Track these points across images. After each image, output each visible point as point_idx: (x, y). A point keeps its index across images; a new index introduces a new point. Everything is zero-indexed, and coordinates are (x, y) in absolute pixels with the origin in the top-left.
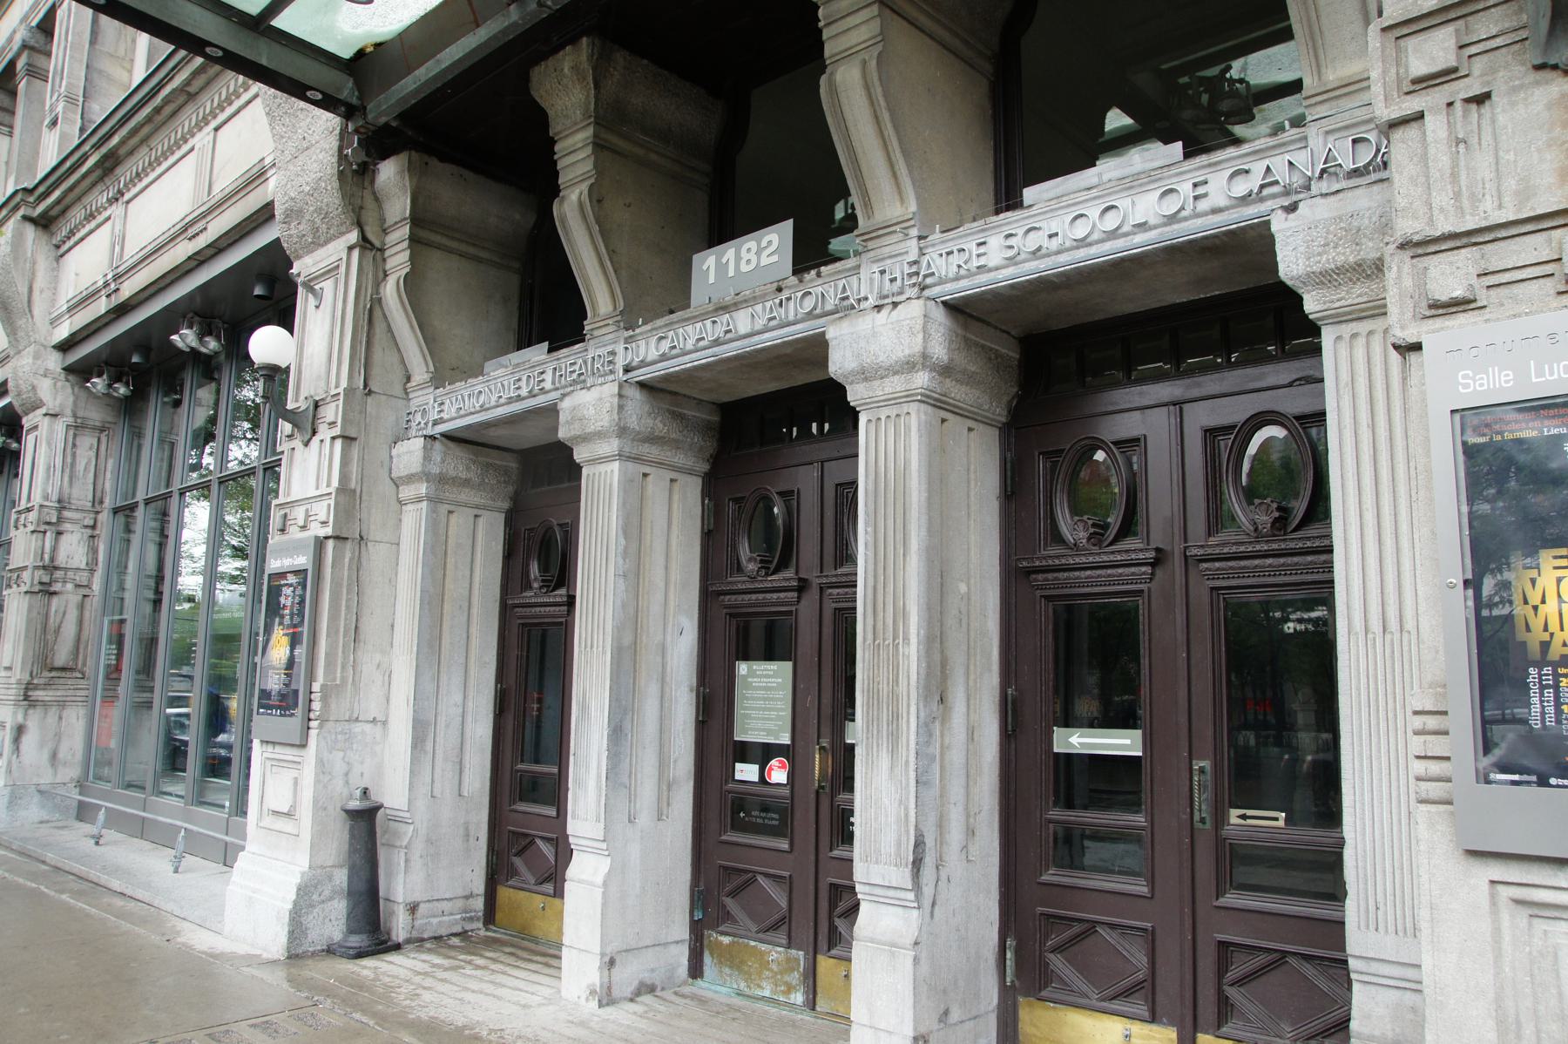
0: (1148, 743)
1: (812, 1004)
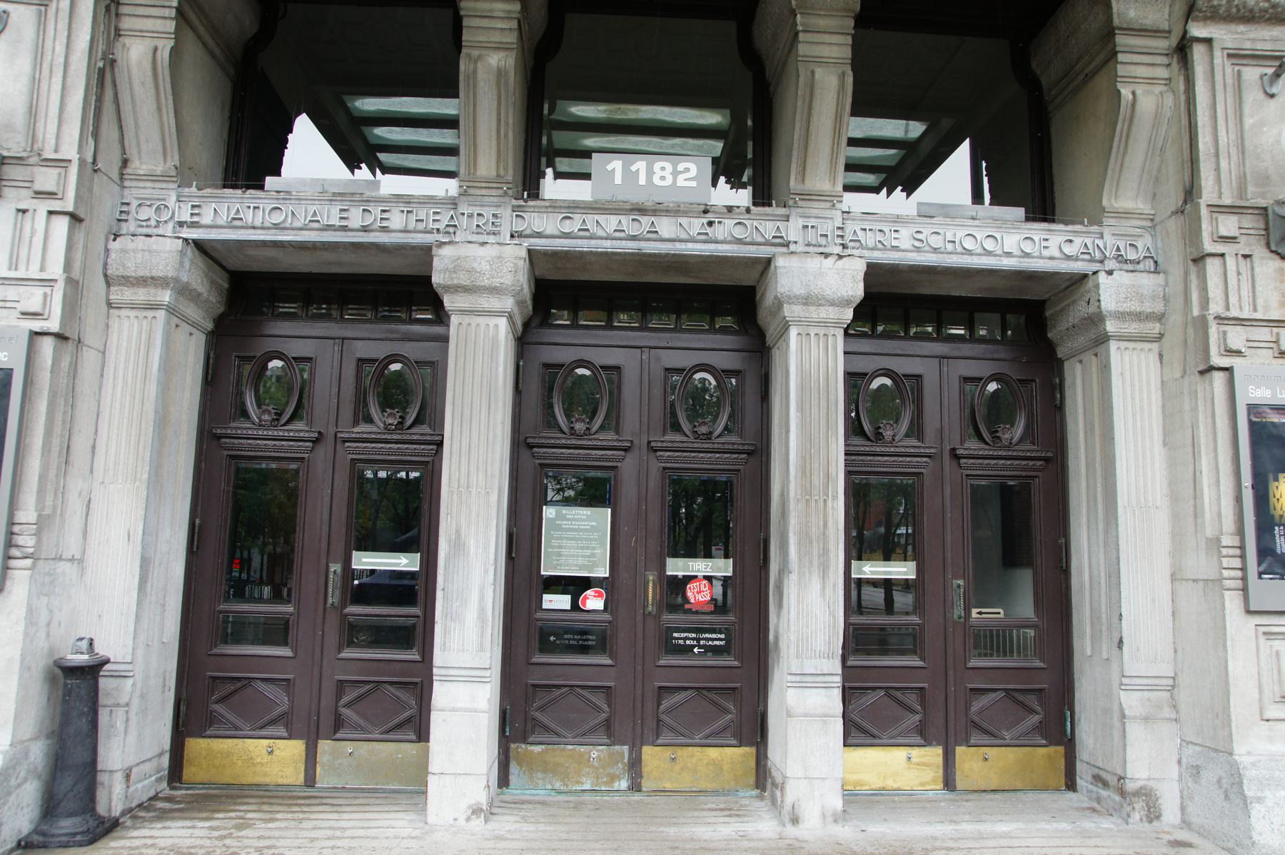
0: (920, 571)
1: (635, 787)
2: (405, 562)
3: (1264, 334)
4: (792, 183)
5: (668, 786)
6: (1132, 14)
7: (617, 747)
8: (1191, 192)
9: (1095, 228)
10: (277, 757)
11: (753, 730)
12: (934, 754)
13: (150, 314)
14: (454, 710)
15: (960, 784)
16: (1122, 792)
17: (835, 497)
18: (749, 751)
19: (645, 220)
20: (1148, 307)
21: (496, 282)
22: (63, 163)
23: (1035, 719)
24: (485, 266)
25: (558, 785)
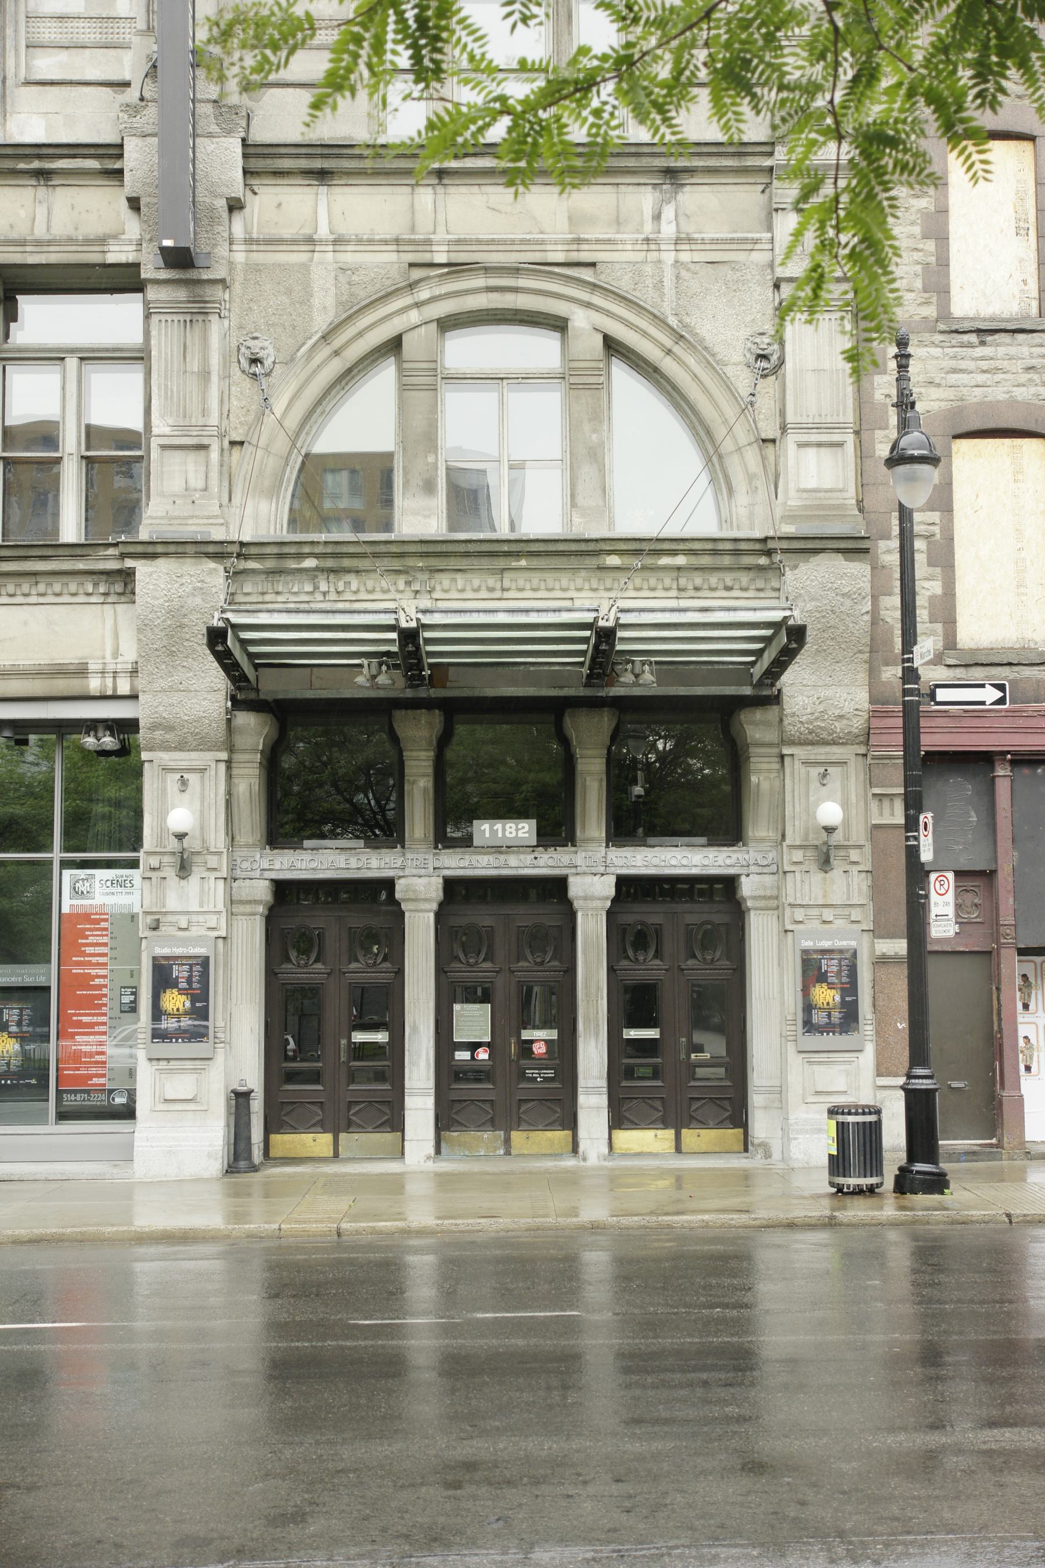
1: (508, 1153)
2: (381, 1037)
3: (815, 912)
6: (757, 736)
8: (783, 836)
10: (320, 1142)
11: (570, 1122)
15: (684, 1150)
18: (569, 1133)
19: (502, 857)
20: (768, 893)
21: (428, 896)
22: (220, 853)
23: (727, 1114)
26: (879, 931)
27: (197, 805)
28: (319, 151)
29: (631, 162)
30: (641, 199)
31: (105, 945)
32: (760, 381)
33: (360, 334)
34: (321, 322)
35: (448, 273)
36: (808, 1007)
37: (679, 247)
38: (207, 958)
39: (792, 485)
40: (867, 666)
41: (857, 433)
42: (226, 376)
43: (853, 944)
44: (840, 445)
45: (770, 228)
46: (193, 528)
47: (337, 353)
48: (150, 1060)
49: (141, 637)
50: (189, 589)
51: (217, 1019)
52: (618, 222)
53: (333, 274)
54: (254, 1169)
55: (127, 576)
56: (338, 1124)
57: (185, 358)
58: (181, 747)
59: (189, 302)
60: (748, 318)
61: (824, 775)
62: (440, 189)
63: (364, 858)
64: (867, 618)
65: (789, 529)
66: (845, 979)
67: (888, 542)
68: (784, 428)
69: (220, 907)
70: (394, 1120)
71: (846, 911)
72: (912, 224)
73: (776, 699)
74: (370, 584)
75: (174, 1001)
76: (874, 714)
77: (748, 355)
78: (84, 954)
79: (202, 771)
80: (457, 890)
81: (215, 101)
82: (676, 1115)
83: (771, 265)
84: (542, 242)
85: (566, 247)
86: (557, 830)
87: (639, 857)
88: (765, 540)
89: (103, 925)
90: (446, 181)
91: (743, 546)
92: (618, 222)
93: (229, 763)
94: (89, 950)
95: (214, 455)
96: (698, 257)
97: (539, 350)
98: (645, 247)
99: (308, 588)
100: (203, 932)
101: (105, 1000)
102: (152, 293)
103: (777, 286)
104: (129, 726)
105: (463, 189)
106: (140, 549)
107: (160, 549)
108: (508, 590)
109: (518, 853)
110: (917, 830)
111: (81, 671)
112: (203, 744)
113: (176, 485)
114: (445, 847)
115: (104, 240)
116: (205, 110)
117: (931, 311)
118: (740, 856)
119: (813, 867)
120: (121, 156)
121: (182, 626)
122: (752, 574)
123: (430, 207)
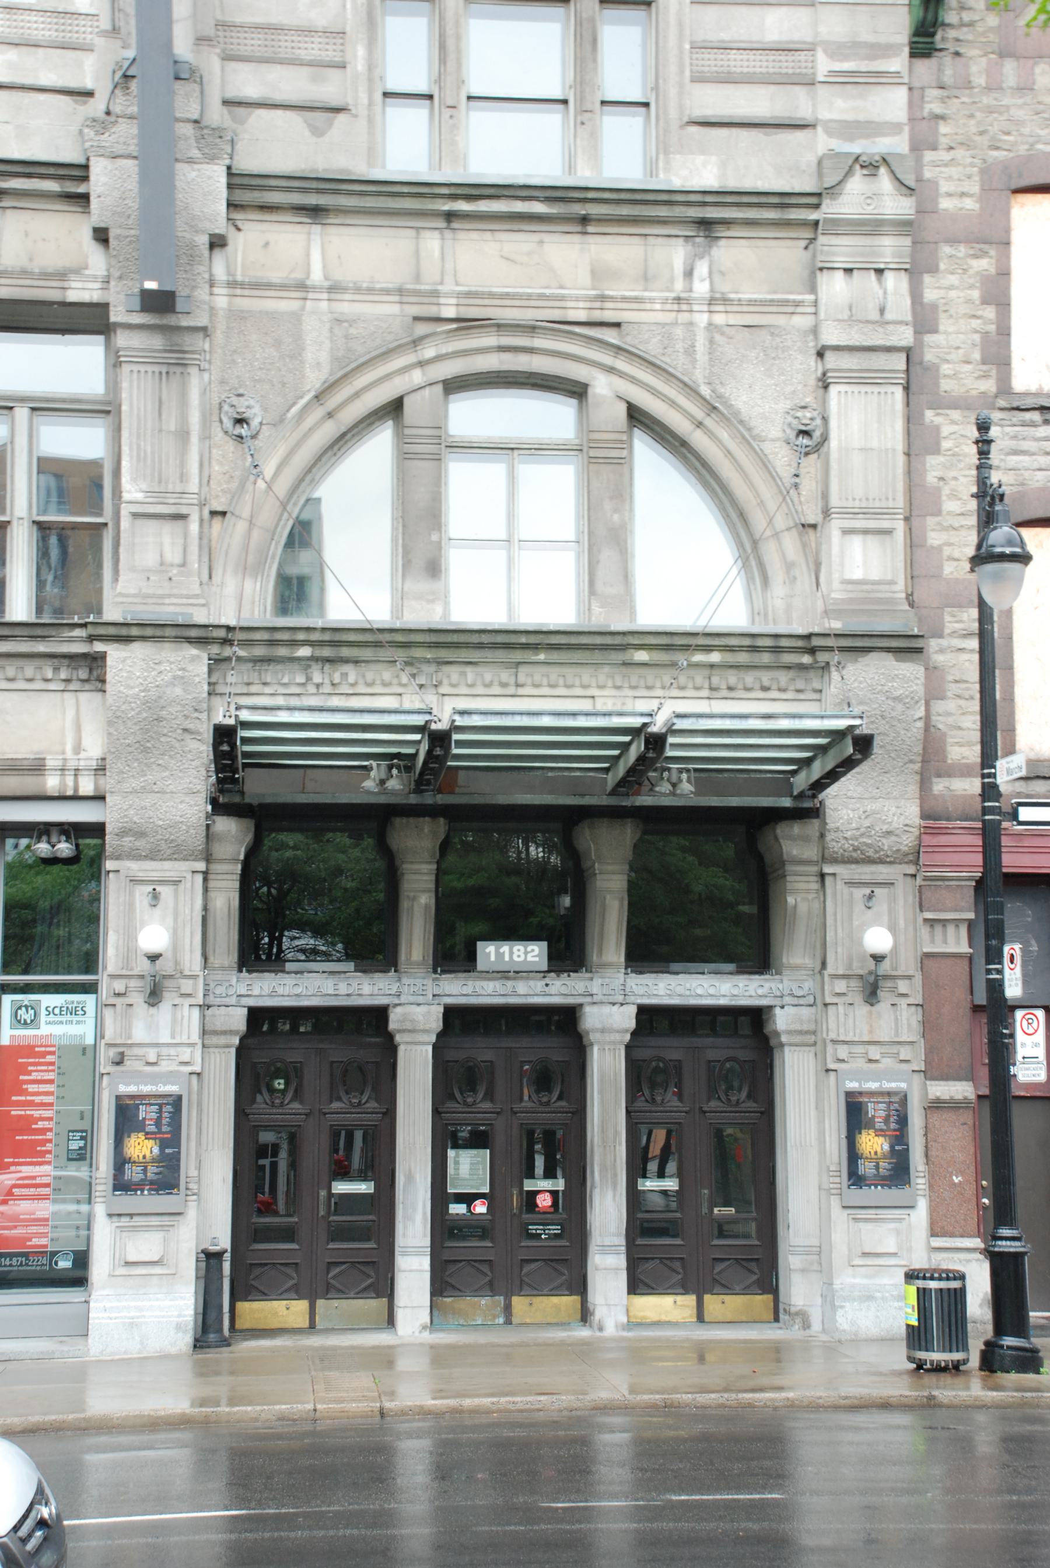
0: (681, 1185)
1: (508, 1322)
3: (860, 1049)
4: (595, 958)
5: (528, 1321)
6: (795, 852)
7: (497, 1298)
8: (824, 964)
9: (778, 977)
10: (292, 1311)
11: (579, 1285)
12: (691, 1300)
13: (227, 1050)
14: (411, 1271)
15: (707, 1318)
16: (790, 1314)
17: (620, 1144)
18: (576, 1299)
19: (510, 983)
20: (805, 1027)
21: (427, 1027)
22: (194, 977)
23: (755, 1277)
24: (421, 1018)
25: (462, 1322)
26: (932, 1072)
27: (170, 920)
28: (314, 185)
29: (662, 212)
30: (673, 253)
31: (51, 1082)
32: (805, 462)
33: (357, 395)
34: (314, 379)
35: (457, 329)
36: (853, 1155)
37: (713, 308)
38: (180, 1098)
39: (836, 576)
40: (918, 777)
41: (907, 519)
42: (206, 437)
43: (903, 1085)
44: (888, 532)
45: (813, 289)
46: (171, 609)
47: (330, 415)
48: (110, 1215)
49: (112, 730)
50: (167, 677)
51: (188, 1168)
52: (646, 278)
53: (328, 326)
54: (226, 1343)
55: (96, 661)
56: (314, 1288)
57: (160, 415)
58: (152, 856)
59: (166, 351)
60: (789, 389)
61: (870, 897)
62: (448, 234)
63: (355, 984)
64: (920, 724)
65: (837, 625)
66: (893, 1126)
67: (940, 641)
68: (826, 513)
69: (195, 1038)
70: (381, 1283)
71: (894, 1049)
72: (971, 287)
73: (816, 813)
74: (370, 676)
75: (141, 1147)
76: (927, 831)
77: (788, 431)
78: (25, 1092)
79: (176, 883)
80: (459, 1020)
81: (196, 122)
82: (696, 1279)
83: (815, 331)
84: (562, 298)
85: (588, 305)
86: (568, 953)
87: (661, 985)
88: (809, 637)
89: (49, 1058)
90: (454, 225)
91: (784, 642)
92: (646, 278)
93: (206, 874)
94: (32, 1088)
95: (194, 527)
96: (733, 319)
97: (551, 417)
98: (676, 307)
99: (300, 679)
100: (174, 1067)
101: (49, 1146)
102: (122, 339)
103: (820, 354)
104: (98, 830)
105: (474, 235)
106: (112, 631)
107: (135, 631)
108: (522, 686)
109: (527, 978)
110: (1001, 963)
111: (38, 768)
112: (178, 853)
113: (149, 558)
114: (444, 972)
115: (65, 275)
116: (187, 130)
117: (989, 386)
118: (773, 985)
119: (858, 999)
120: (85, 179)
121: (159, 720)
122: (791, 674)
123: (437, 253)
